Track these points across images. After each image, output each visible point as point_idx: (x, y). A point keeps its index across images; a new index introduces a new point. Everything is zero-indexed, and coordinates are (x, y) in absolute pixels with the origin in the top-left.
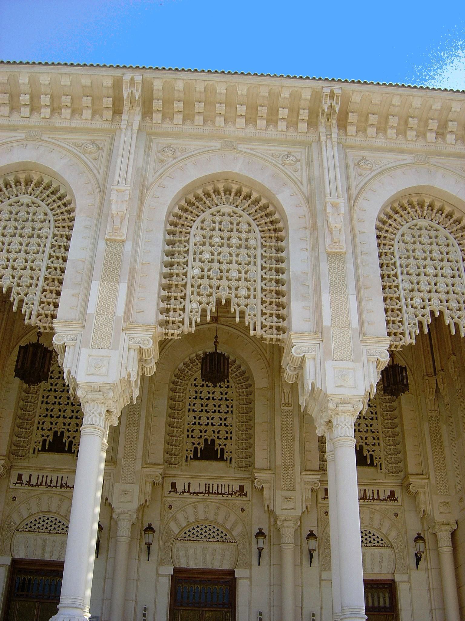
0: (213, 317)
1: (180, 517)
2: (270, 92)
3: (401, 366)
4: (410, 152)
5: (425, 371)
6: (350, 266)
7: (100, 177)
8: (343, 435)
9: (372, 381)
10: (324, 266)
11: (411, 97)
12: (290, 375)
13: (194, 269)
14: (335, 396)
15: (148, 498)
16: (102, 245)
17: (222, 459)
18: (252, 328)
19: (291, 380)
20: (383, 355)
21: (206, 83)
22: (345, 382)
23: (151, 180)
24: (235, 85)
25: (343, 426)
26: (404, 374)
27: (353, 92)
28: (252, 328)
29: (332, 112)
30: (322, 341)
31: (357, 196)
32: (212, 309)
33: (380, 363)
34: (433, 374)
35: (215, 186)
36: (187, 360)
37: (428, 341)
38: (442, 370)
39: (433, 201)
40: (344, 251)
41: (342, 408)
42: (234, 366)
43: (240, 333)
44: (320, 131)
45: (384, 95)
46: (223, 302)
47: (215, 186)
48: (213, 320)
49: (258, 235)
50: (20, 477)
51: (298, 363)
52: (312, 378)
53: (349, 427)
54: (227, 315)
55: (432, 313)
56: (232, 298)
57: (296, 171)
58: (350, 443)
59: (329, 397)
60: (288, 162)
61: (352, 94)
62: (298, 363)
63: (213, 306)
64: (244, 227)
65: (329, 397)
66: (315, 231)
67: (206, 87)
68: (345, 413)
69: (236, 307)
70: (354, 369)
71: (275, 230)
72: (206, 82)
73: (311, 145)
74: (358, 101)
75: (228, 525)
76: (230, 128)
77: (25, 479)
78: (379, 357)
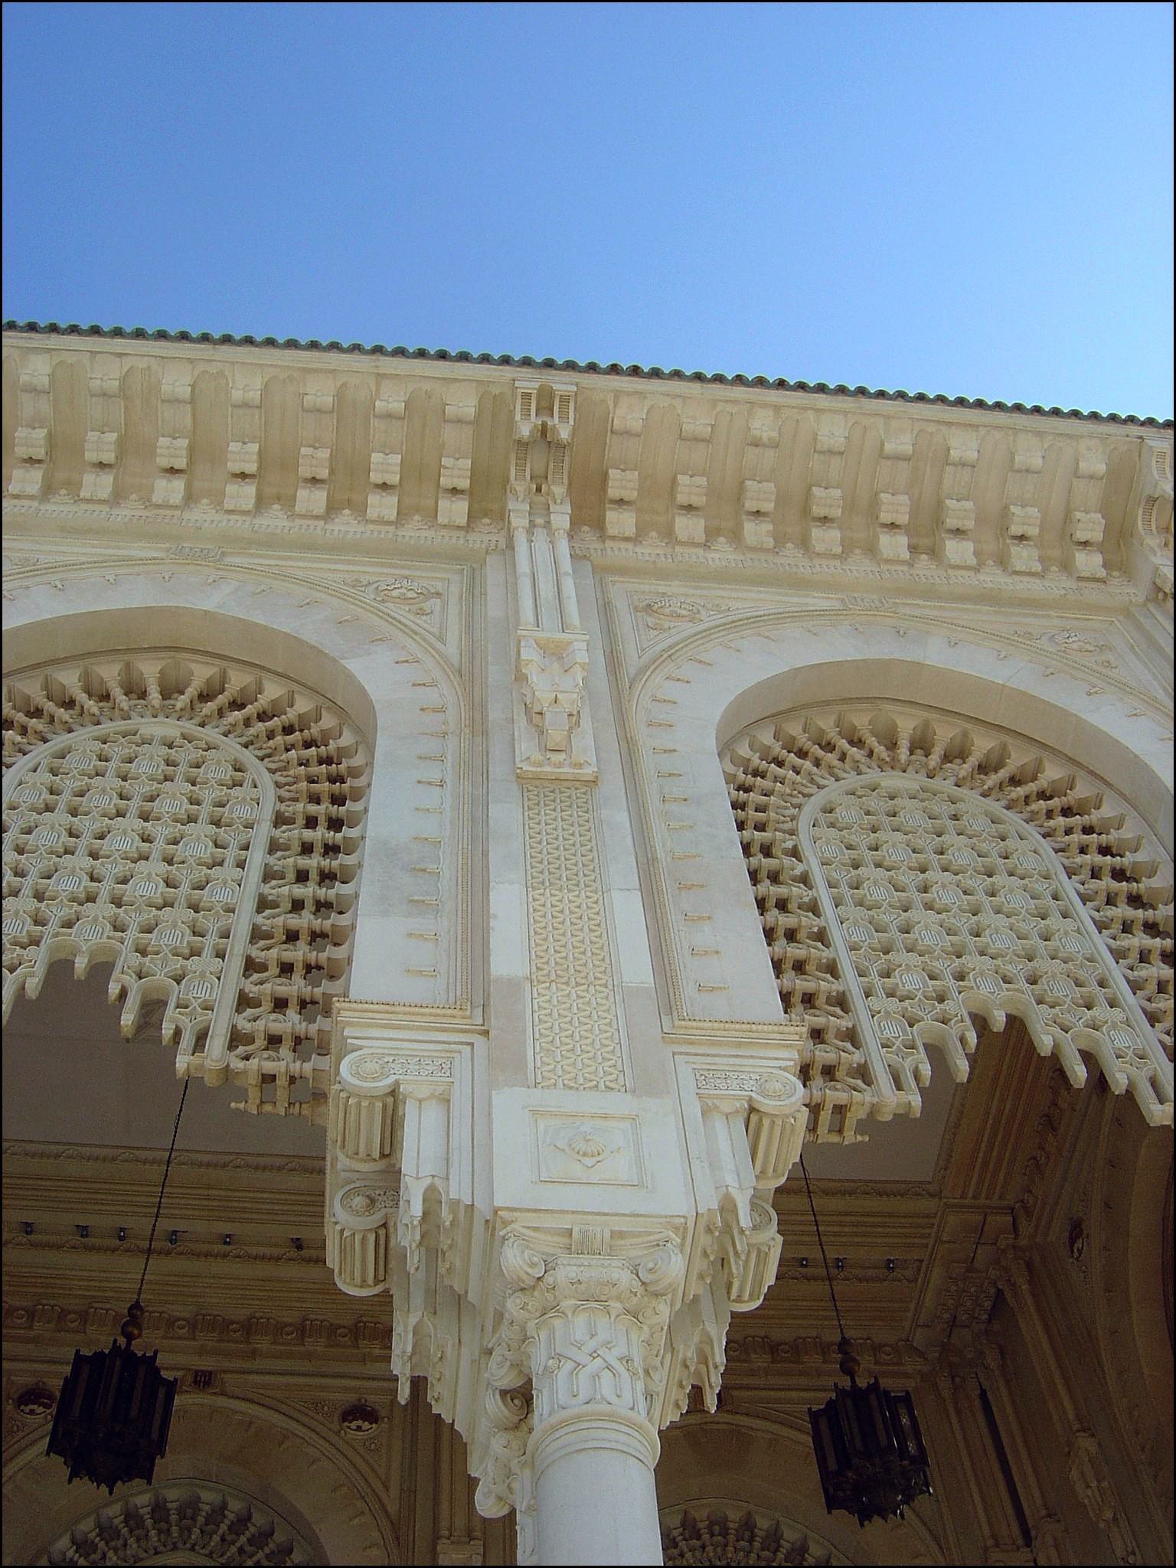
0: (197, 1372)
2: (339, 395)
3: (886, 1393)
4: (829, 587)
5: (987, 1532)
6: (618, 817)
8: (581, 1398)
9: (730, 1180)
11: (811, 415)
12: (346, 1234)
14: (532, 1220)
18: (187, 1041)
19: (358, 1280)
20: (778, 1086)
21: (128, 363)
22: (590, 1161)
24: (221, 374)
25: (583, 1358)
26: (905, 1421)
27: (618, 394)
28: (187, 1041)
29: (551, 465)
30: (486, 1033)
32: (24, 983)
33: (766, 1122)
34: (1020, 1542)
35: (128, 665)
36: (87, 1526)
37: (985, 1431)
38: (1049, 1516)
39: (926, 724)
40: (588, 771)
41: (572, 1272)
42: (267, 1550)
43: (293, 1425)
44: (511, 508)
45: (720, 407)
46: (81, 964)
47: (128, 665)
48: (196, 1382)
51: (369, 1142)
52: (427, 1170)
53: (620, 1368)
54: (247, 1365)
55: (981, 1022)
56: (120, 952)
57: (421, 612)
58: (622, 1437)
59: (506, 1223)
60: (395, 593)
61: (615, 406)
62: (369, 1142)
63: (32, 975)
64: (217, 771)
65: (506, 1223)
66: (478, 739)
67: (124, 379)
68: (594, 1298)
69: (130, 980)
70: (633, 1119)
71: (328, 761)
72: (125, 360)
73: (483, 564)
74: (636, 425)
76: (203, 514)
78: (753, 1095)
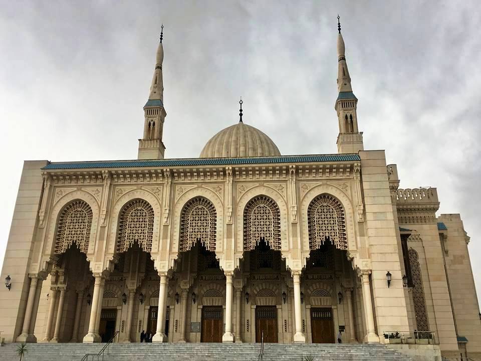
1: (257, 288)
7: (222, 200)
10: (291, 228)
13: (253, 229)
15: (246, 283)
16: (226, 226)
17: (270, 267)
23: (238, 200)
31: (302, 200)
49: (272, 214)
50: (202, 277)
75: (273, 290)
77: (204, 278)
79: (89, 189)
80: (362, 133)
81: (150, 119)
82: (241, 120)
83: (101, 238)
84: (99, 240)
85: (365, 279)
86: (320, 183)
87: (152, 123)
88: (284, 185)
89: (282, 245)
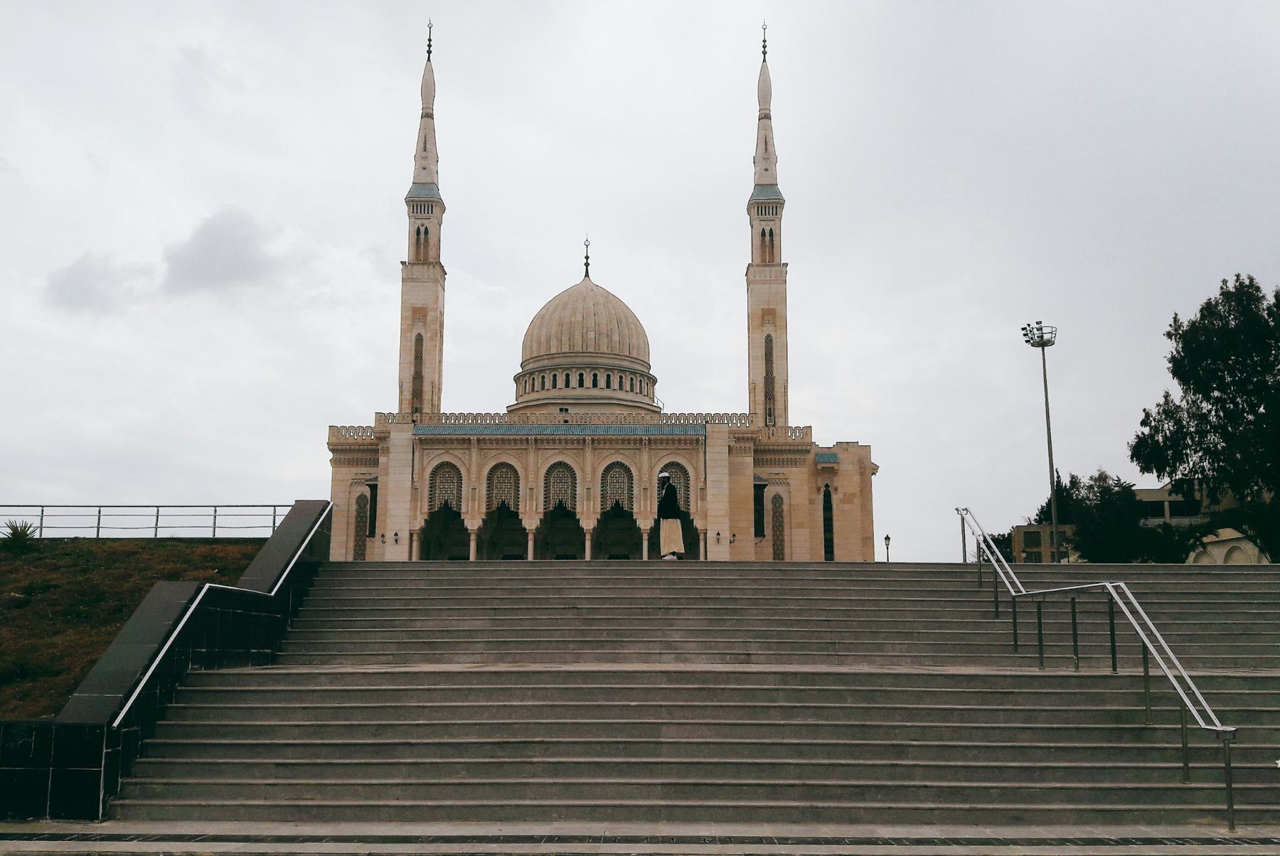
16: (585, 490)
23: (596, 466)
79: (456, 452)
80: (787, 264)
81: (419, 222)
82: (587, 275)
83: (473, 499)
84: (472, 500)
85: (702, 537)
86: (670, 452)
87: (422, 230)
88: (637, 451)
89: (634, 507)
